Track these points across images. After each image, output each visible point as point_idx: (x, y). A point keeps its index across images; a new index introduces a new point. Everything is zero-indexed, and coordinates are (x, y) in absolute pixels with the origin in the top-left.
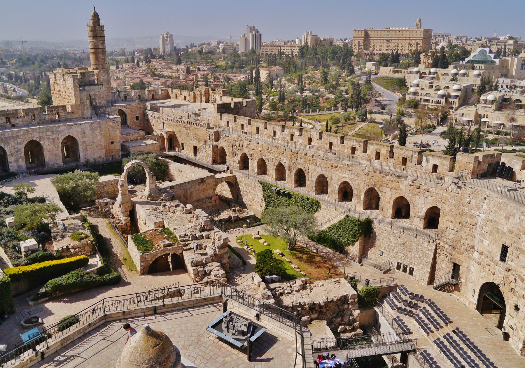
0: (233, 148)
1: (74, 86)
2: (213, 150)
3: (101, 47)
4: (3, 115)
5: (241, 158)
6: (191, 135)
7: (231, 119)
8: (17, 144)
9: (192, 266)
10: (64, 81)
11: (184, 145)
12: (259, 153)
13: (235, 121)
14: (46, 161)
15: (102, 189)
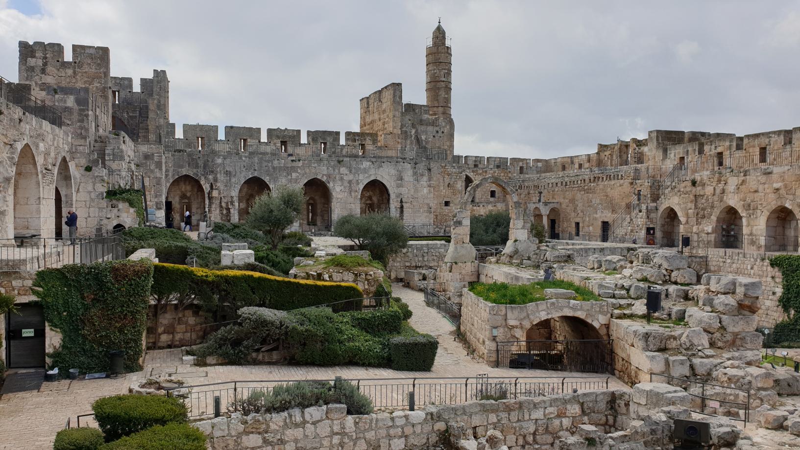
0: (696, 202)
1: (394, 101)
2: (648, 217)
3: (444, 79)
4: (278, 137)
5: (718, 221)
6: (596, 201)
7: (690, 149)
8: (290, 181)
9: (646, 349)
10: (380, 101)
11: (581, 225)
12: (772, 196)
13: (701, 152)
14: (333, 219)
15: (421, 259)
